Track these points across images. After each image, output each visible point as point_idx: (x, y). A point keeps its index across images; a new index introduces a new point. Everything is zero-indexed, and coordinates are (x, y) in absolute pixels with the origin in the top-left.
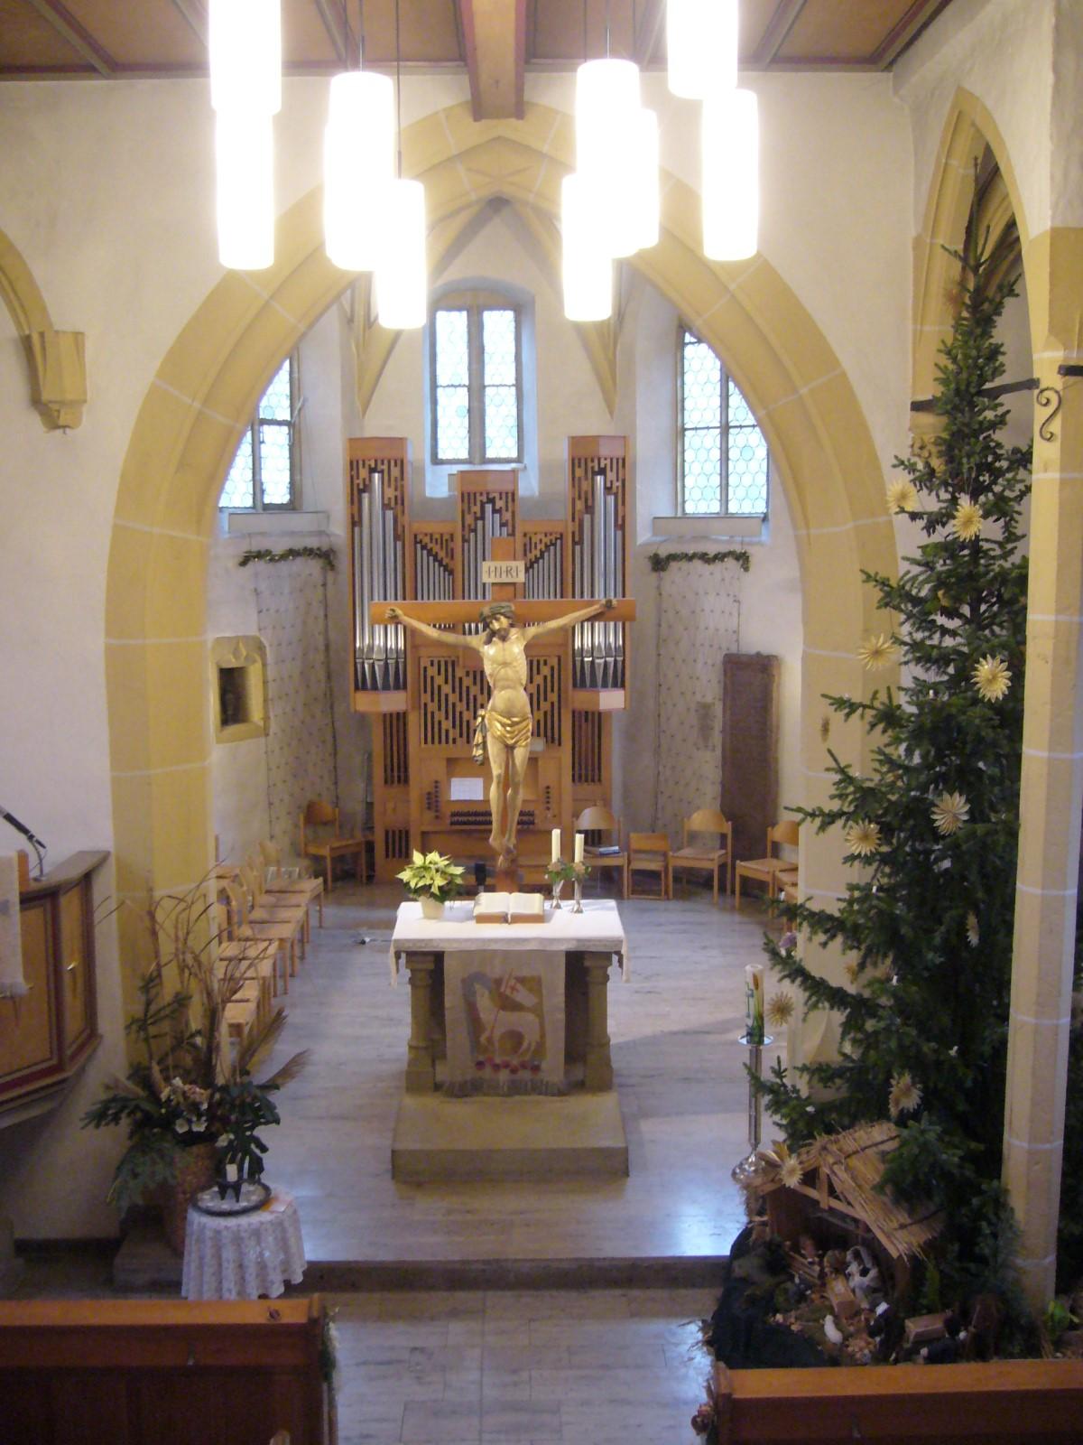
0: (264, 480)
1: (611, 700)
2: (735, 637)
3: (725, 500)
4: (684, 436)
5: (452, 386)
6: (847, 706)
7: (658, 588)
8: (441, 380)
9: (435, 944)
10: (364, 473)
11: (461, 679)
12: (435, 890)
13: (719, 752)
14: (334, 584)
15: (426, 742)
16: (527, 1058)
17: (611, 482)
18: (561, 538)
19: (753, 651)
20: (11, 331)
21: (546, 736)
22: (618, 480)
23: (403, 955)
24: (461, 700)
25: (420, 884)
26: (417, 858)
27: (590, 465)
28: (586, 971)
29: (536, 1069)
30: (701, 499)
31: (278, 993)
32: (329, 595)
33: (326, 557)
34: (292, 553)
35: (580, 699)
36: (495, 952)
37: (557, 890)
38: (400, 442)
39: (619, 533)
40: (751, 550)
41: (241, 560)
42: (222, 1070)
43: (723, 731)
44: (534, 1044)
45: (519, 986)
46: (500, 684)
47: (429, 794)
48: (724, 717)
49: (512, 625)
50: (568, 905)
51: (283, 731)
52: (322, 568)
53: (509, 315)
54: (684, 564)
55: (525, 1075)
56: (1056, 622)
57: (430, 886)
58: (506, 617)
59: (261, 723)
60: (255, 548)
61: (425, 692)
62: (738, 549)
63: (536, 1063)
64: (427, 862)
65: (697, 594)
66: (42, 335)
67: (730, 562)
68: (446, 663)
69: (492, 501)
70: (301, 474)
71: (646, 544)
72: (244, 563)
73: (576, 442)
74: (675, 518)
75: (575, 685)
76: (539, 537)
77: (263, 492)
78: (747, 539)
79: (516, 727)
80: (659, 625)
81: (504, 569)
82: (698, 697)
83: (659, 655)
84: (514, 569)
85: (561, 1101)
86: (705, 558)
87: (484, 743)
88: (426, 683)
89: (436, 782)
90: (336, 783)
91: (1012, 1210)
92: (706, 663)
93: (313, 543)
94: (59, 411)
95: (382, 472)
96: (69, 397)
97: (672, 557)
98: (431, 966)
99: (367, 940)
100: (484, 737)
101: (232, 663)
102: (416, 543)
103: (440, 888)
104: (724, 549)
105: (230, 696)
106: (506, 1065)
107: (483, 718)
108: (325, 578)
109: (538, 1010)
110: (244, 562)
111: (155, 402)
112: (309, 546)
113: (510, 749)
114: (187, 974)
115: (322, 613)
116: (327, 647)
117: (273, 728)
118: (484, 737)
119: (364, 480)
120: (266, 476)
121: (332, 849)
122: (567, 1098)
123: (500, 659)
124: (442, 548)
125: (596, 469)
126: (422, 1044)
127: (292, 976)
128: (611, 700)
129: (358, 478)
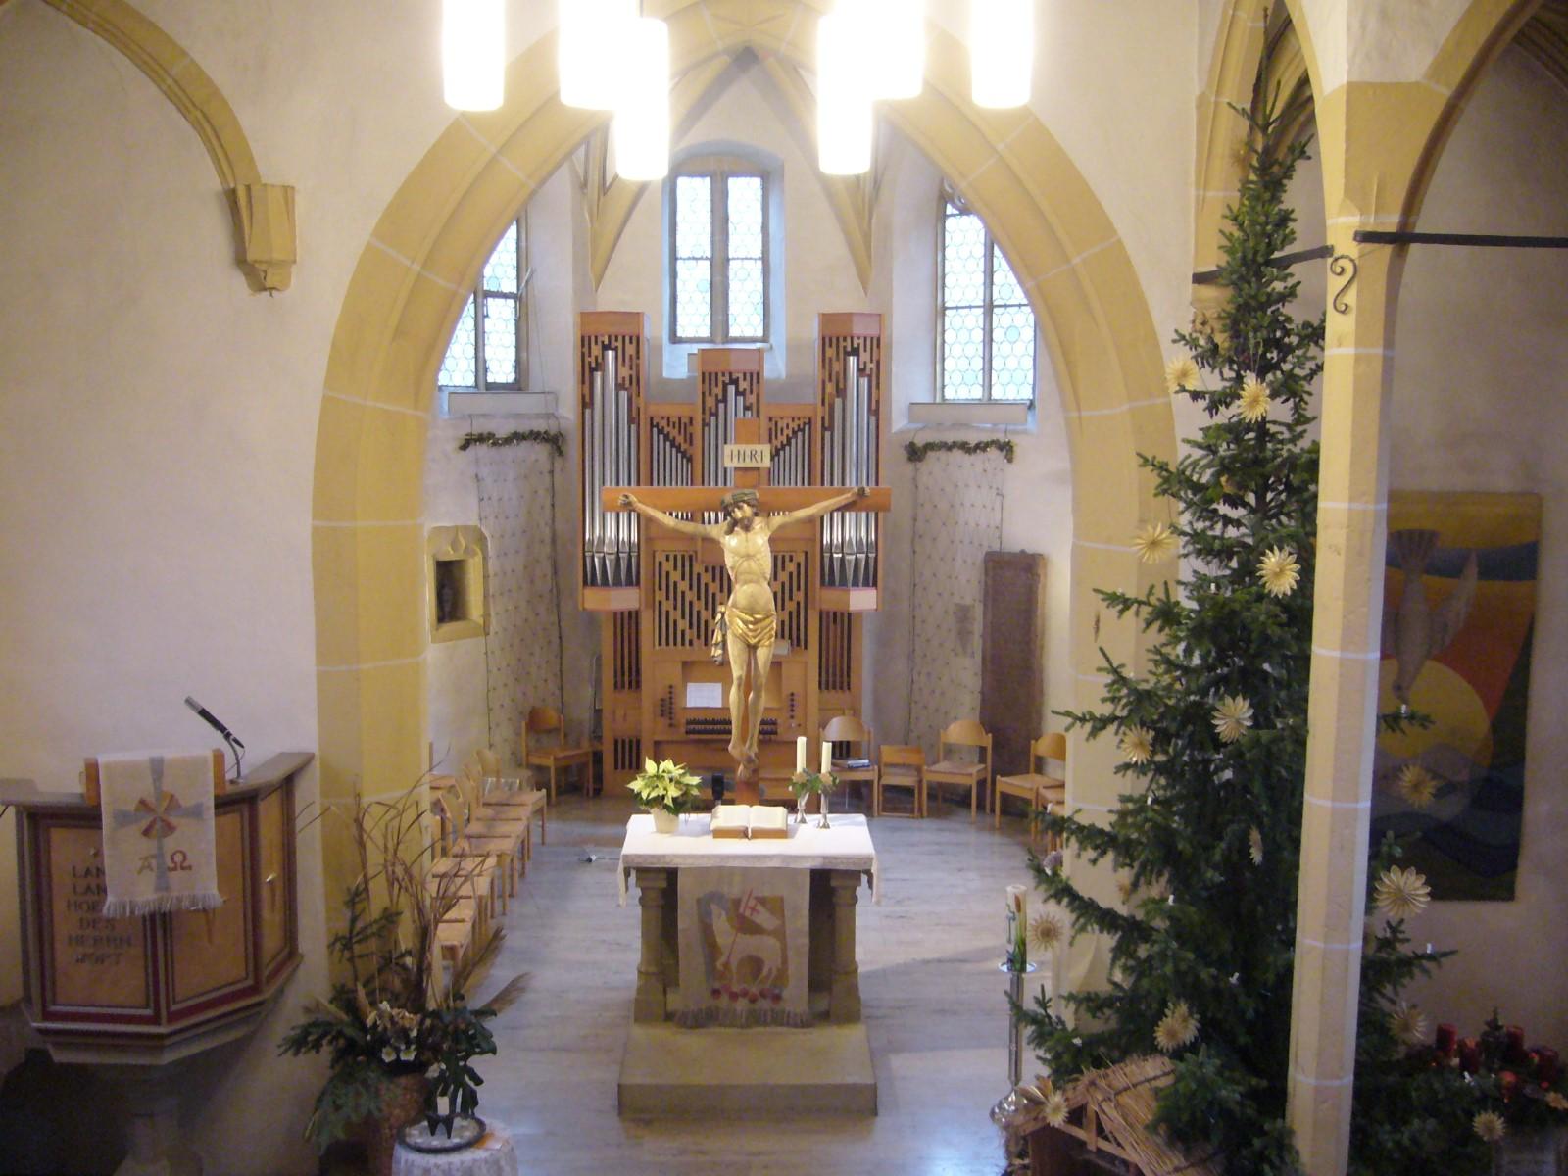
0: (487, 356)
1: (862, 600)
2: (997, 534)
3: (988, 386)
4: (944, 315)
5: (694, 258)
6: (1123, 603)
7: (915, 479)
8: (682, 252)
9: (668, 860)
10: (596, 350)
12: (668, 801)
13: (978, 657)
14: (562, 470)
15: (660, 644)
16: (768, 985)
17: (865, 363)
18: (810, 423)
19: (1016, 548)
20: (215, 184)
21: (790, 637)
22: (872, 361)
23: (633, 874)
24: (699, 598)
25: (653, 795)
26: (650, 766)
27: (842, 344)
28: (832, 891)
29: (777, 998)
30: (961, 384)
31: (495, 915)
33: (554, 441)
34: (517, 437)
35: (828, 599)
36: (732, 869)
37: (802, 803)
38: (636, 317)
39: (873, 418)
40: (1015, 440)
41: (463, 442)
42: (434, 995)
43: (982, 636)
44: (775, 972)
45: (759, 907)
46: (742, 578)
47: (663, 700)
49: (756, 514)
50: (813, 820)
51: (505, 630)
53: (756, 182)
54: (943, 454)
55: (765, 1004)
56: (1350, 510)
57: (663, 797)
58: (748, 504)
59: (481, 621)
60: (476, 431)
61: (660, 589)
62: (1002, 438)
63: (777, 991)
64: (661, 771)
65: (956, 486)
66: (248, 188)
67: (992, 452)
68: (683, 557)
69: (735, 382)
71: (901, 432)
72: (464, 447)
73: (827, 319)
75: (823, 583)
76: (785, 422)
77: (486, 370)
78: (1011, 428)
79: (759, 625)
80: (915, 520)
81: (748, 453)
82: (957, 599)
83: (914, 552)
84: (759, 453)
85: (804, 1034)
86: (965, 447)
87: (724, 642)
88: (661, 579)
89: (671, 687)
91: (1297, 1152)
92: (965, 561)
93: (540, 426)
94: (265, 272)
95: (616, 349)
96: (277, 255)
97: (930, 446)
98: (664, 884)
99: (594, 858)
100: (724, 636)
101: (449, 555)
102: (652, 426)
103: (674, 799)
104: (985, 438)
105: (446, 591)
106: (745, 994)
107: (723, 614)
109: (780, 934)
110: (465, 446)
111: (370, 267)
112: (536, 430)
113: (752, 648)
114: (396, 886)
116: (553, 541)
117: (494, 627)
118: (724, 636)
119: (596, 358)
120: (489, 353)
121: (555, 759)
122: (811, 1030)
123: (743, 551)
125: (849, 349)
126: (652, 969)
127: (511, 895)
128: (862, 600)
129: (590, 356)
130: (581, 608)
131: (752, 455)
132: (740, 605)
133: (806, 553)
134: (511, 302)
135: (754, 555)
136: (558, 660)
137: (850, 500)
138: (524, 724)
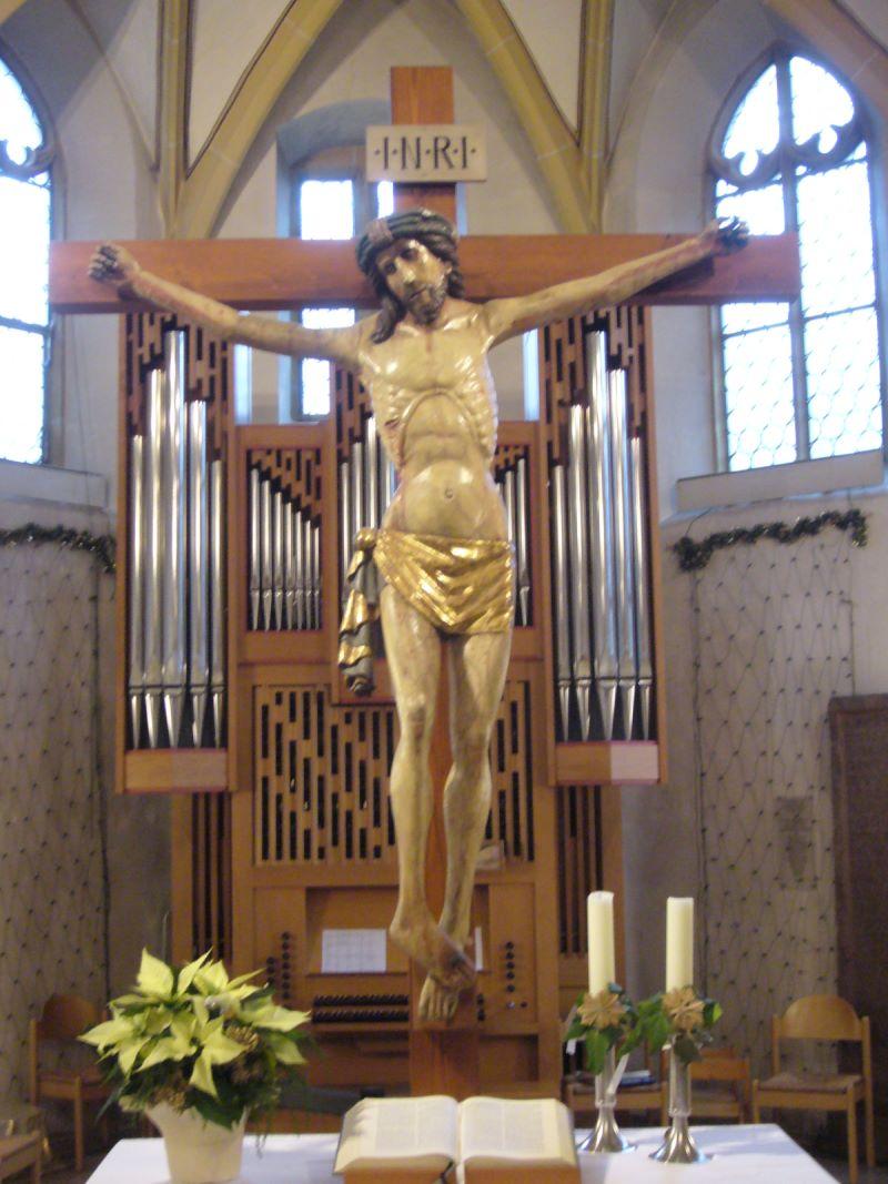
1: (633, 763)
2: (845, 669)
3: (804, 443)
4: (722, 348)
7: (693, 599)
10: (151, 334)
11: (334, 730)
12: (201, 1079)
13: (826, 888)
15: (265, 855)
18: (526, 456)
21: (503, 836)
22: (630, 345)
24: (335, 770)
25: (152, 1059)
26: (153, 976)
32: (103, 615)
35: (570, 763)
37: (606, 1092)
39: (636, 442)
40: (865, 508)
47: (271, 961)
48: (836, 815)
49: (454, 289)
50: (641, 1143)
52: (95, 570)
54: (740, 551)
57: (188, 1064)
61: (265, 754)
62: (842, 508)
64: (182, 988)
68: (306, 696)
70: (63, 415)
74: (715, 475)
75: (559, 738)
78: (856, 492)
79: (475, 577)
80: (697, 665)
81: (427, 144)
82: (780, 790)
84: (456, 144)
86: (779, 533)
87: (375, 627)
88: (266, 737)
90: (107, 965)
93: (77, 522)
97: (718, 541)
100: (372, 608)
102: (249, 468)
103: (221, 1073)
104: (813, 513)
107: (369, 550)
108: (97, 587)
113: (449, 640)
115: (88, 649)
118: (372, 608)
119: (152, 347)
121: (85, 1086)
123: (421, 377)
124: (298, 479)
128: (633, 763)
129: (141, 344)
130: (119, 789)
131: (440, 151)
132: (412, 523)
133: (527, 685)
134: (38, 339)
135: (449, 386)
136: (101, 916)
137: (701, 254)
138: (33, 1023)
